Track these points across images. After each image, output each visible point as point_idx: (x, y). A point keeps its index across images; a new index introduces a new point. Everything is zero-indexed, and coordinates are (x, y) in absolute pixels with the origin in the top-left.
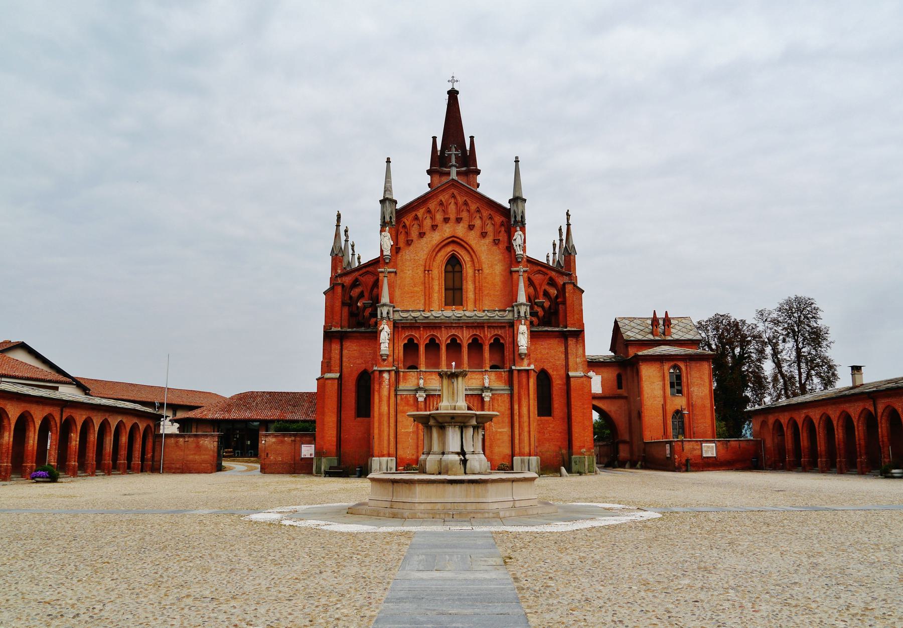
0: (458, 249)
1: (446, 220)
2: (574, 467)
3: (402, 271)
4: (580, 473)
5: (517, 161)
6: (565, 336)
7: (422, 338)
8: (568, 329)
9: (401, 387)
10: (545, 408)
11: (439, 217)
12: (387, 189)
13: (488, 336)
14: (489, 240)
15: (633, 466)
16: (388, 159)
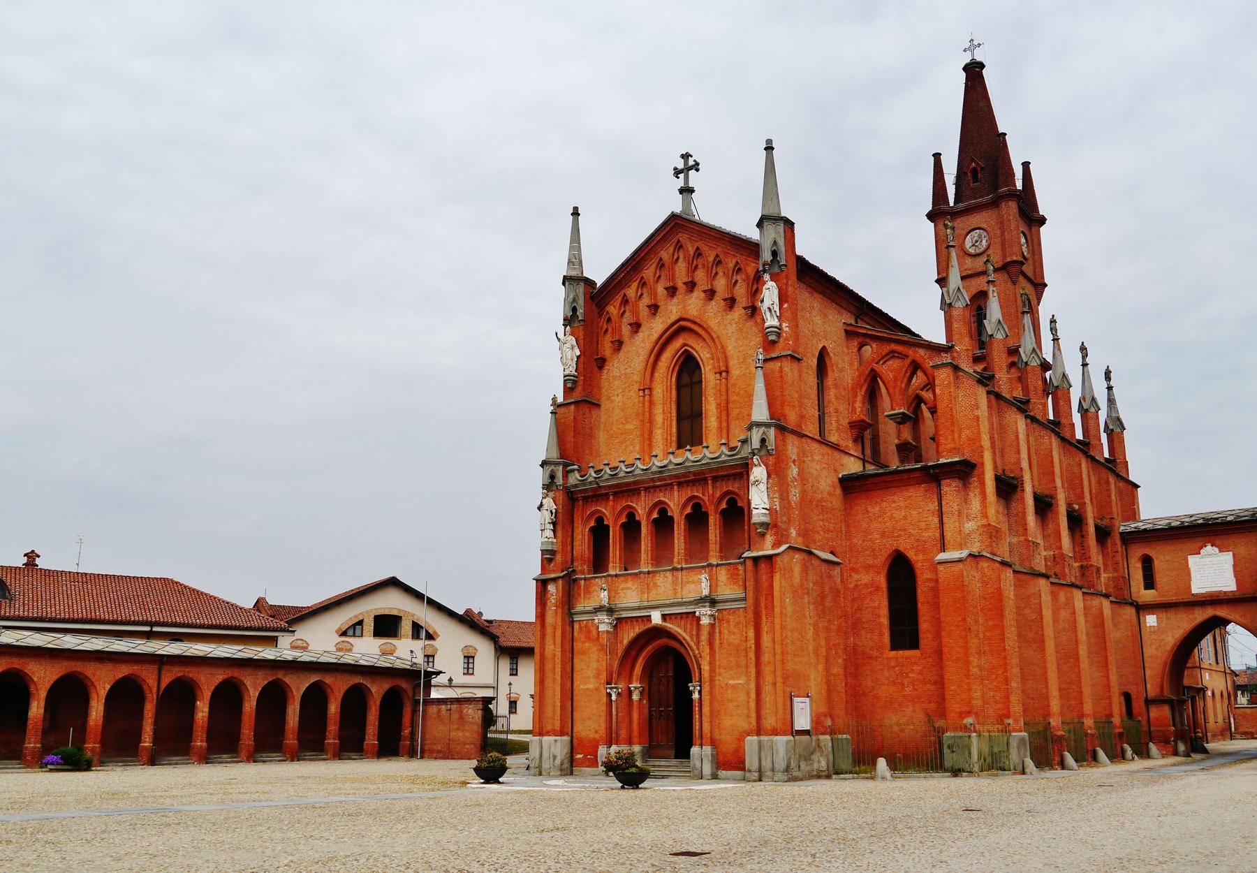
0: (692, 341)
1: (672, 291)
2: (949, 759)
3: (609, 398)
4: (956, 772)
5: (769, 148)
6: (934, 476)
7: (610, 512)
8: (942, 461)
9: (579, 608)
10: (905, 631)
11: (660, 289)
12: (575, 259)
13: (709, 495)
14: (738, 312)
15: (1087, 757)
16: (576, 209)
